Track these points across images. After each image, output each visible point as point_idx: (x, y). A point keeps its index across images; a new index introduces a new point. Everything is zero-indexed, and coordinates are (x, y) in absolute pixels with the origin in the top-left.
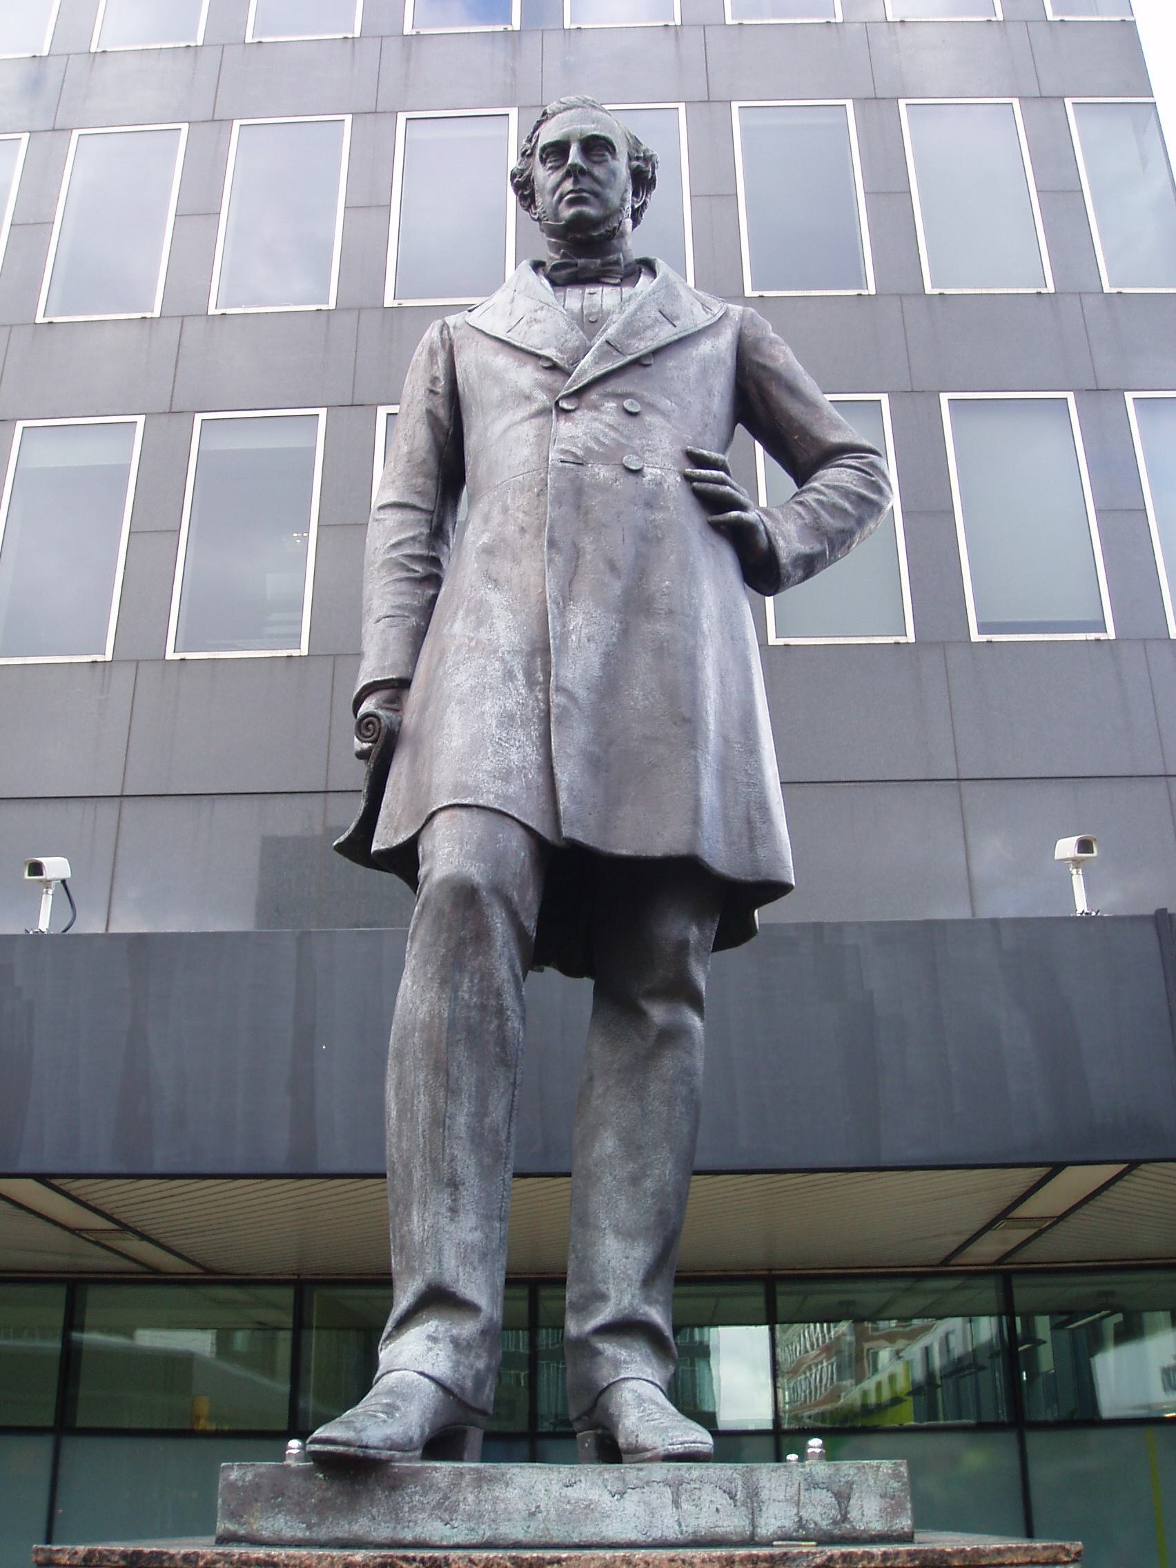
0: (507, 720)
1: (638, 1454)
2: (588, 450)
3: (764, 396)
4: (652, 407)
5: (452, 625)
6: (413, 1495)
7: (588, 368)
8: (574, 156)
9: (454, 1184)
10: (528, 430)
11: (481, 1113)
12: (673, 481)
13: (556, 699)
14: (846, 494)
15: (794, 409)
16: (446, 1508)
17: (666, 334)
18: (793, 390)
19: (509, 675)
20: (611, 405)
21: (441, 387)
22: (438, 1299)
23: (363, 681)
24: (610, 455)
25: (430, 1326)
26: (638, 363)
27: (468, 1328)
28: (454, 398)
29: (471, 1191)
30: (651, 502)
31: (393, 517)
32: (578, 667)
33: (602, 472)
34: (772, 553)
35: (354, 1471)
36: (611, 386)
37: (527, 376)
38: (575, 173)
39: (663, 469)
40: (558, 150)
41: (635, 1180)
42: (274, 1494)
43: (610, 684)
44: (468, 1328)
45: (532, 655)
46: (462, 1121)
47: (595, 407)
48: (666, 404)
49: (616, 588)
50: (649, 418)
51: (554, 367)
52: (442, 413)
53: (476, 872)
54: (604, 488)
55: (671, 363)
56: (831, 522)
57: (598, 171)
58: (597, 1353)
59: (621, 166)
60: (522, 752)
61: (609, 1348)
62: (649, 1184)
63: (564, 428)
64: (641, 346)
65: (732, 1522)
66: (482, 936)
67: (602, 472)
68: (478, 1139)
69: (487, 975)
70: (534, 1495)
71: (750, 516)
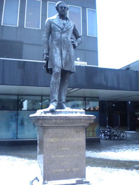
0: (59, 59)
2: (65, 38)
3: (75, 32)
8: (63, 9)
10: (59, 34)
13: (63, 58)
15: (77, 33)
18: (77, 31)
19: (59, 56)
20: (66, 33)
21: (50, 26)
22: (55, 101)
26: (68, 29)
31: (46, 38)
33: (66, 39)
34: (75, 46)
37: (59, 29)
40: (62, 7)
41: (64, 93)
45: (60, 54)
46: (57, 89)
47: (65, 33)
51: (61, 29)
52: (50, 29)
53: (59, 72)
54: (66, 41)
56: (79, 43)
57: (65, 10)
58: (62, 104)
59: (66, 9)
60: (60, 62)
61: (63, 104)
62: (65, 93)
63: (63, 35)
64: (69, 28)
66: (59, 76)
67: (66, 39)
71: (75, 43)
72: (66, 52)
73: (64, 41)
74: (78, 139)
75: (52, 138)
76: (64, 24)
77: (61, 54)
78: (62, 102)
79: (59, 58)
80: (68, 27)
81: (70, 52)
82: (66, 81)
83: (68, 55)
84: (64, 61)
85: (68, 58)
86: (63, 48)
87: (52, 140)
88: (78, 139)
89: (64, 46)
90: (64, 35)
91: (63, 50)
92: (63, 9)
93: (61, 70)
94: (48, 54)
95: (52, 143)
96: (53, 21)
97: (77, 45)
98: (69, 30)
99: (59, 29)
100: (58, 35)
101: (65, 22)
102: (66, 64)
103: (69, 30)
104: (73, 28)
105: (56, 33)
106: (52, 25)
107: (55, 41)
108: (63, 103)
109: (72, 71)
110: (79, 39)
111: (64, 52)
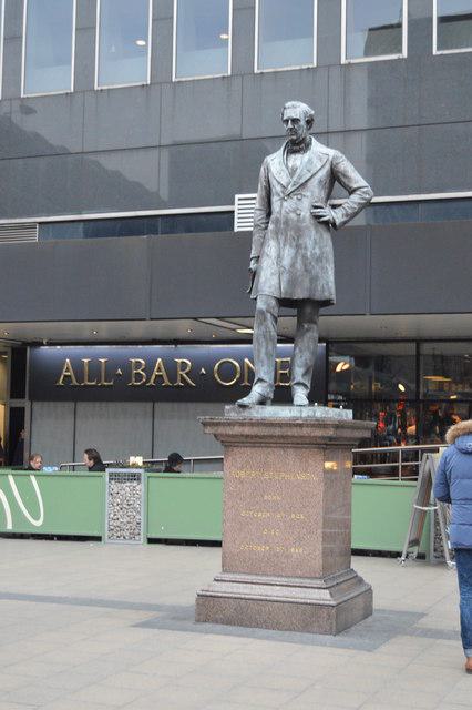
6: (252, 411)
7: (290, 188)
9: (262, 362)
11: (267, 348)
12: (308, 215)
15: (345, 181)
16: (257, 412)
22: (260, 380)
24: (294, 211)
25: (259, 384)
27: (265, 384)
29: (266, 362)
31: (258, 212)
32: (286, 262)
33: (293, 215)
35: (243, 407)
37: (279, 188)
39: (306, 213)
42: (233, 410)
43: (293, 265)
46: (263, 350)
48: (309, 194)
49: (294, 244)
50: (304, 199)
55: (309, 184)
56: (350, 211)
60: (275, 281)
63: (285, 204)
64: (302, 181)
66: (265, 319)
67: (293, 215)
68: (267, 353)
69: (266, 327)
72: (293, 251)
73: (287, 222)
74: (302, 477)
75: (242, 468)
76: (292, 172)
77: (279, 257)
81: (306, 248)
82: (306, 326)
83: (299, 260)
84: (285, 277)
85: (299, 265)
87: (242, 474)
91: (284, 245)
92: (290, 125)
93: (273, 302)
97: (345, 219)
98: (303, 185)
101: (297, 160)
102: (293, 282)
103: (303, 185)
104: (323, 174)
108: (298, 384)
109: (318, 296)
111: (286, 251)
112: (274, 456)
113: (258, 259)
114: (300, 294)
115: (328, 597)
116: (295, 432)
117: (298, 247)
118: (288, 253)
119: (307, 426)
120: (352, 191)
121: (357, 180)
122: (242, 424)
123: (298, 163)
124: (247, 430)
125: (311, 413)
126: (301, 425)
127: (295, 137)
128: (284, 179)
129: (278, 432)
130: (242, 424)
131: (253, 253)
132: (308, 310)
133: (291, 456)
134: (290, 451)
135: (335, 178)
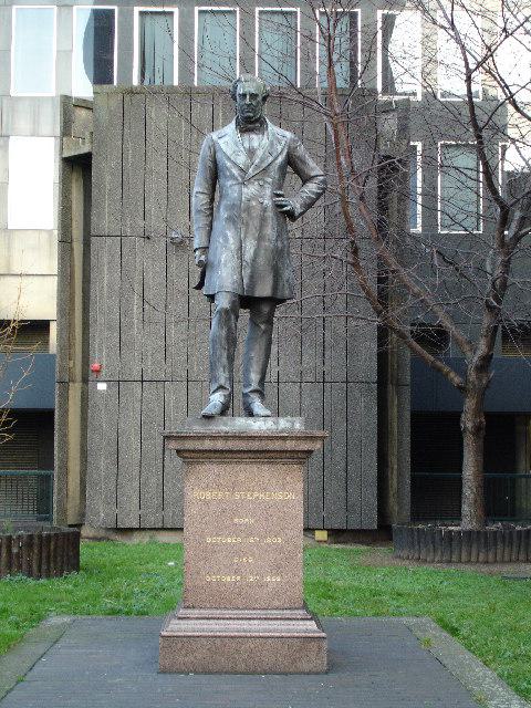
1: (258, 415)
4: (265, 182)
5: (218, 240)
14: (313, 193)
16: (225, 424)
17: (271, 159)
22: (221, 387)
23: (196, 246)
28: (215, 162)
30: (265, 210)
31: (201, 196)
32: (248, 255)
35: (208, 417)
36: (257, 177)
37: (235, 172)
38: (248, 105)
39: (268, 202)
40: (244, 95)
44: (227, 393)
56: (308, 201)
63: (245, 190)
64: (264, 165)
65: (274, 427)
66: (229, 319)
70: (240, 423)
73: (248, 209)
74: (279, 496)
76: (251, 152)
78: (252, 388)
79: (236, 262)
80: (262, 161)
84: (246, 273)
85: (261, 261)
86: (246, 233)
87: (208, 495)
88: (279, 496)
89: (247, 225)
90: (250, 190)
94: (205, 249)
95: (206, 503)
96: (221, 142)
99: (235, 172)
100: (231, 189)
101: (255, 140)
105: (229, 183)
106: (219, 155)
107: (226, 208)
109: (279, 296)
110: (312, 187)
112: (246, 472)
113: (205, 249)
114: (264, 290)
115: (315, 627)
116: (277, 445)
117: (260, 239)
118: (250, 248)
119: (292, 438)
120: (306, 179)
121: (314, 168)
122: (213, 438)
123: (255, 144)
124: (220, 445)
125: (288, 425)
126: (284, 438)
127: (251, 115)
128: (242, 159)
129: (255, 445)
130: (213, 438)
131: (196, 243)
132: (266, 309)
133: (265, 472)
134: (265, 467)
135: (292, 163)
